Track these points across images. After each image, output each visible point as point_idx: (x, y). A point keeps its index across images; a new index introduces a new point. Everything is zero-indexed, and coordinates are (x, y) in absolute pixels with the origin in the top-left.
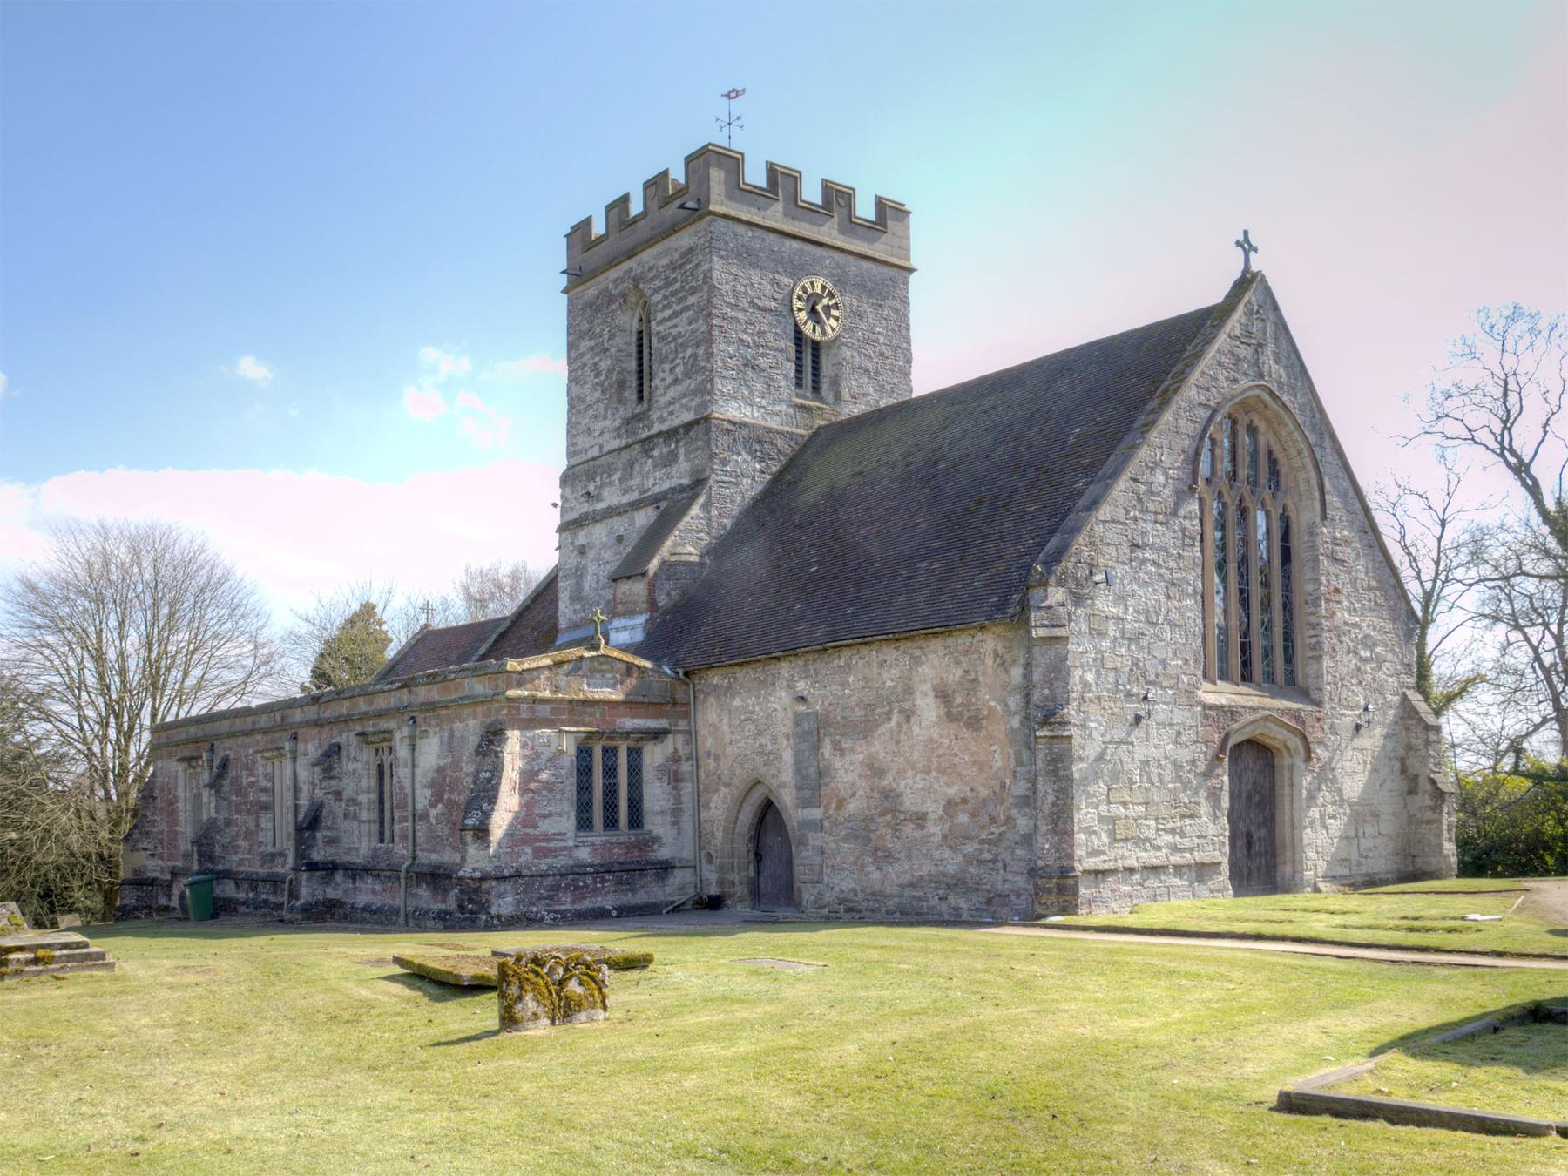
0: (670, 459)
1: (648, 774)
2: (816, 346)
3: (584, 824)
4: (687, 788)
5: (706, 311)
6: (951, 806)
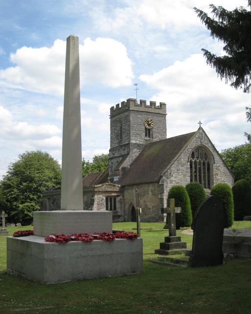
0: (124, 150)
1: (117, 202)
2: (149, 130)
3: (107, 209)
4: (123, 204)
5: (129, 126)
6: (153, 207)
